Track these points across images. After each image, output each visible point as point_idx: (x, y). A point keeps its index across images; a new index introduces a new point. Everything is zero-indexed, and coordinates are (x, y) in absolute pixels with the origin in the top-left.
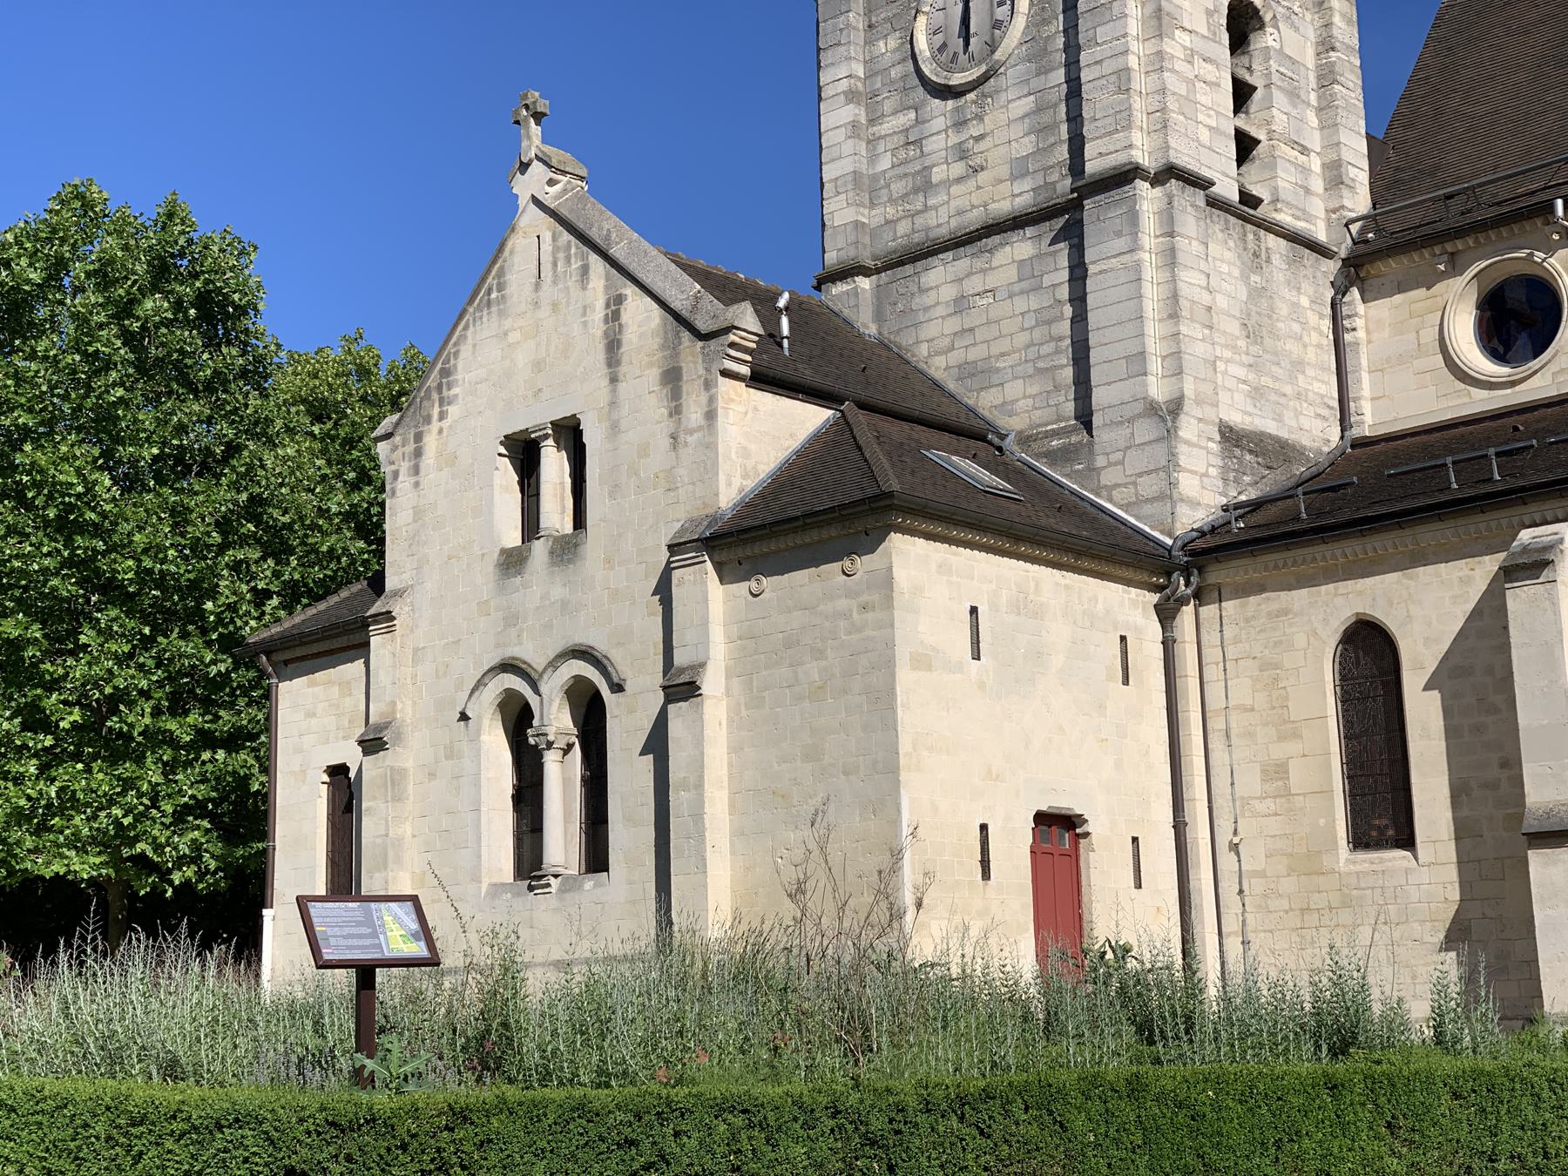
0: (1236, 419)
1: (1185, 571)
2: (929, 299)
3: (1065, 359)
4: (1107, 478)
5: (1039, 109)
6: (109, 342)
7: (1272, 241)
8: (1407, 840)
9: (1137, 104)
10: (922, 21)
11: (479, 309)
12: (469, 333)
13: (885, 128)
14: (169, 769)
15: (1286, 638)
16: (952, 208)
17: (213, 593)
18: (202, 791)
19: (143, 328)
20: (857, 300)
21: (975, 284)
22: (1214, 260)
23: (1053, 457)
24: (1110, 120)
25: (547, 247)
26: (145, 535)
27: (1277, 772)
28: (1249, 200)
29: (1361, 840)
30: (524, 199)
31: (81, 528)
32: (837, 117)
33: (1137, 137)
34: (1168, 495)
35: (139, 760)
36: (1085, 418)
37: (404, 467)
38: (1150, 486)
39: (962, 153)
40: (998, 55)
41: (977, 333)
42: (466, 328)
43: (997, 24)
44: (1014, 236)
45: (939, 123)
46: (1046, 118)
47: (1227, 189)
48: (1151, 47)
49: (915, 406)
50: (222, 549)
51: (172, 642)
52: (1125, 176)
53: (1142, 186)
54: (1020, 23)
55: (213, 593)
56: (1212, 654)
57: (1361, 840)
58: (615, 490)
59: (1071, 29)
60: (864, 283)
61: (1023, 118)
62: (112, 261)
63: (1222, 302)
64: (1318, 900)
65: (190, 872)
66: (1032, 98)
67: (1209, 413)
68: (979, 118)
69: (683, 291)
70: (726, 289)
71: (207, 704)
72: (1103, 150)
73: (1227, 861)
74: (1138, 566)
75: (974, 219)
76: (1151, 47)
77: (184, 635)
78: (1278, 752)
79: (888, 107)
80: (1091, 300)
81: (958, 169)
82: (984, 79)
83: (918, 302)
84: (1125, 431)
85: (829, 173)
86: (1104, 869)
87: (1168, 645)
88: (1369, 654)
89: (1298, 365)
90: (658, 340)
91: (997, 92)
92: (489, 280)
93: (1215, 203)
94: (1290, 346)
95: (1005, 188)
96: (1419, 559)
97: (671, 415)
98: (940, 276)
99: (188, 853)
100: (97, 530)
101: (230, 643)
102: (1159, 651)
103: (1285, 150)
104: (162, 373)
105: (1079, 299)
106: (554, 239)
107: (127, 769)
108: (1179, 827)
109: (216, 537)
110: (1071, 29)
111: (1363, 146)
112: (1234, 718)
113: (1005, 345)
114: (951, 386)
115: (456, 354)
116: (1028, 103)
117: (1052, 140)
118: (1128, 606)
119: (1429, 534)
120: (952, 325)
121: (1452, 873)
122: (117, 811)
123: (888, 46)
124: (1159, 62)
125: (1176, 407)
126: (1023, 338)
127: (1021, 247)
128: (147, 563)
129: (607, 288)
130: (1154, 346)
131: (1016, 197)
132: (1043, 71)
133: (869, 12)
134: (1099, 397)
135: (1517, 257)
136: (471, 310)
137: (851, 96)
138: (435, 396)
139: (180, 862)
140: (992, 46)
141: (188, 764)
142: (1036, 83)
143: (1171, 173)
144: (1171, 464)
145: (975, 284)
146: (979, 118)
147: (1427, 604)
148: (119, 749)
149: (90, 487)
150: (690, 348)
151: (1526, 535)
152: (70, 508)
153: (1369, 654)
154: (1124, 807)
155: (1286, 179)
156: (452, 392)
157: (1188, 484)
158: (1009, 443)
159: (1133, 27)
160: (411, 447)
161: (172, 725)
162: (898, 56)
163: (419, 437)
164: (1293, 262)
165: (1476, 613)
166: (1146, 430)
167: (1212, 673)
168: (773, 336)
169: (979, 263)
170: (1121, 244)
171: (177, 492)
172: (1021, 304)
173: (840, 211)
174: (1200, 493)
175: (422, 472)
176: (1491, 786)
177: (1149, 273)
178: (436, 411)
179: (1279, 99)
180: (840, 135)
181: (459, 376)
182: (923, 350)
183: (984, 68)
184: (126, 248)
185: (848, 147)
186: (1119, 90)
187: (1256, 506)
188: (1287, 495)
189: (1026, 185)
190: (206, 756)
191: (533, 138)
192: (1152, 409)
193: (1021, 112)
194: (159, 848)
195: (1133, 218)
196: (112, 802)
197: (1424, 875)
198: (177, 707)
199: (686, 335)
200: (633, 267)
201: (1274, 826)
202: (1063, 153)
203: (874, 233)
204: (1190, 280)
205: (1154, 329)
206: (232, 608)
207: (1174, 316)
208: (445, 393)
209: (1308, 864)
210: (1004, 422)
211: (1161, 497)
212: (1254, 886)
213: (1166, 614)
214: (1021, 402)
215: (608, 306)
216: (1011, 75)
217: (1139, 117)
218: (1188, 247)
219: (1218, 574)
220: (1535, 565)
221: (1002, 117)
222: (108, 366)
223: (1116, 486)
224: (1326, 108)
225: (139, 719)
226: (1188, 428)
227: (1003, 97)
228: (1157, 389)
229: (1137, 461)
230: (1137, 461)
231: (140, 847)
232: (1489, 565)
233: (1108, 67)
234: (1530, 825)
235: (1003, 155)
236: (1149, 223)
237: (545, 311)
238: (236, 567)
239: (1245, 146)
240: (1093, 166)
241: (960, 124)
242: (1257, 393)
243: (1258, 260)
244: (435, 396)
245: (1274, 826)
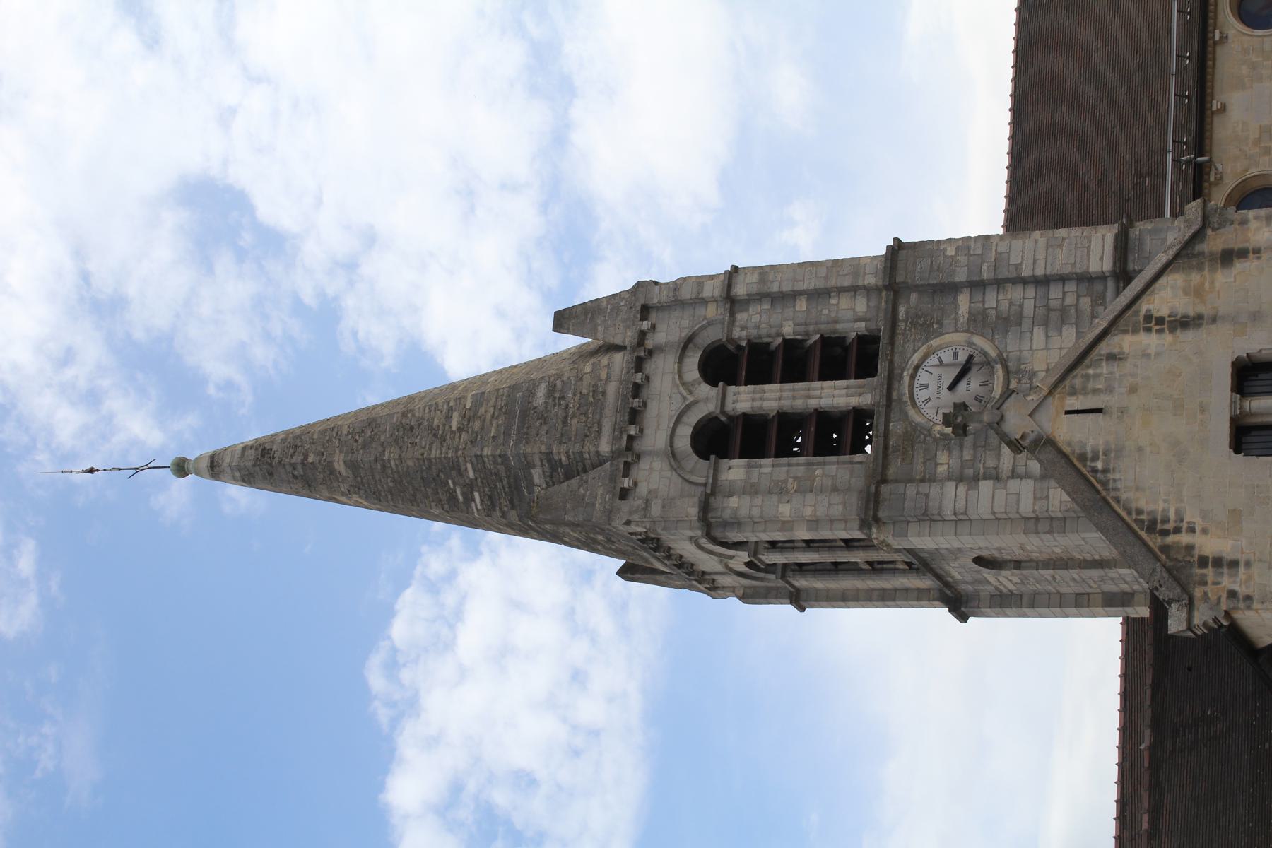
5: (1046, 323)
11: (1104, 484)
12: (1124, 496)
24: (1079, 253)
37: (1227, 582)
40: (993, 353)
42: (1118, 500)
61: (1047, 337)
66: (1036, 329)
68: (1034, 374)
72: (1098, 256)
91: (1019, 359)
92: (1084, 470)
97: (1259, 258)
106: (1073, 393)
115: (1139, 512)
116: (1039, 333)
117: (1073, 311)
129: (1135, 331)
136: (1104, 493)
138: (1171, 539)
146: (1034, 374)
156: (1172, 516)
160: (1209, 572)
162: (956, 453)
163: (1203, 562)
175: (1238, 556)
178: (1184, 538)
180: (1000, 494)
181: (1160, 506)
183: (999, 367)
186: (1060, 246)
193: (1043, 339)
199: (1199, 247)
208: (1170, 526)
215: (1148, 330)
216: (1012, 345)
227: (1026, 354)
244: (1171, 539)
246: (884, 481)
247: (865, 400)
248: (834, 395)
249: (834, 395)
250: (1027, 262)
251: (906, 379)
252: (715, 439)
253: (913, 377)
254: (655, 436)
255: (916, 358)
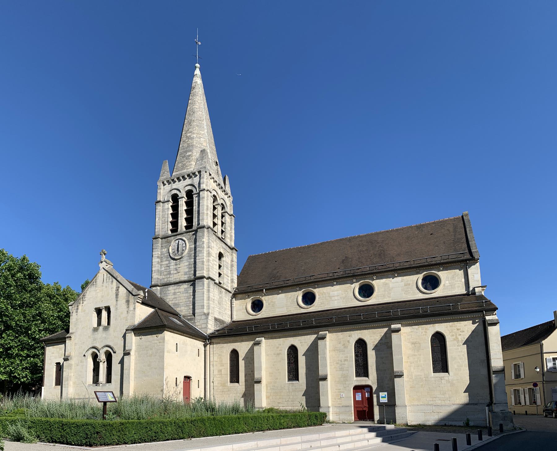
0: (216, 317)
1: (209, 340)
2: (169, 292)
3: (191, 304)
4: (197, 324)
5: (189, 265)
6: (11, 281)
7: (223, 290)
8: (238, 382)
9: (205, 267)
10: (171, 247)
13: (164, 263)
14: (21, 361)
15: (222, 352)
16: (174, 278)
17: (30, 330)
18: (28, 365)
19: (17, 279)
20: (157, 291)
21: (177, 291)
22: (215, 291)
23: (189, 320)
25: (105, 276)
26: (17, 317)
27: (220, 371)
28: (220, 283)
29: (231, 382)
30: (101, 268)
31: (5, 315)
32: (155, 260)
33: (205, 272)
34: (206, 328)
35: (14, 358)
36: (194, 314)
38: (204, 326)
39: (176, 270)
41: (177, 298)
43: (183, 250)
44: (184, 284)
45: (173, 264)
46: (190, 266)
47: (217, 281)
48: (207, 258)
49: (167, 309)
50: (33, 321)
51: (22, 337)
52: (202, 277)
53: (205, 279)
54: (187, 251)
55: (30, 330)
56: (211, 352)
57: (231, 382)
58: (116, 319)
59: (195, 253)
60: (158, 288)
62: (11, 266)
63: (215, 298)
64: (225, 390)
65: (25, 379)
67: (213, 315)
69: (131, 287)
70: (139, 288)
71: (28, 350)
73: (212, 384)
74: (201, 338)
75: (178, 280)
76: (207, 258)
77: (24, 337)
78: (221, 368)
79: (164, 260)
80: (196, 296)
81: (175, 272)
82: (181, 258)
83: (167, 292)
84: (200, 317)
85: (153, 269)
86: (194, 384)
87: (205, 351)
88: (234, 354)
89: (226, 309)
90: (125, 295)
93: (215, 283)
94: (225, 306)
95: (183, 276)
96: (242, 341)
98: (171, 288)
99: (24, 376)
100: (7, 316)
101: (34, 339)
102: (203, 352)
103: (225, 276)
104: (22, 288)
105: (194, 295)
107: (12, 360)
108: (205, 379)
109: (32, 319)
110: (195, 253)
111: (236, 277)
112: (214, 363)
113: (181, 301)
114: (172, 306)
116: (187, 263)
118: (199, 344)
119: (244, 337)
120: (173, 297)
121: (244, 387)
122: (11, 368)
123: (165, 250)
124: (208, 261)
125: (208, 314)
126: (184, 300)
127: (185, 286)
128: (18, 323)
130: (205, 304)
131: (185, 278)
132: (190, 259)
133: (162, 244)
134: (196, 311)
135: (258, 297)
137: (158, 257)
139: (23, 378)
140: (182, 253)
141: (24, 360)
142: (189, 260)
143: (209, 278)
144: (207, 323)
145: (177, 291)
147: (243, 347)
148: (10, 356)
149: (7, 308)
150: (131, 298)
151: (257, 339)
152: (3, 311)
153: (234, 354)
154: (197, 376)
155: (225, 281)
157: (209, 326)
158: (181, 317)
159: (205, 255)
161: (22, 353)
164: (226, 293)
165: (250, 349)
166: (203, 317)
167: (211, 355)
168: (145, 297)
169: (178, 287)
170: (201, 288)
171: (24, 310)
172: (184, 295)
173: (155, 276)
174: (211, 328)
176: (250, 374)
177: (205, 293)
179: (225, 268)
182: (168, 300)
184: (14, 264)
185: (157, 265)
187: (218, 331)
188: (223, 329)
189: (187, 276)
190: (29, 359)
191: (104, 258)
192: (205, 314)
194: (19, 375)
195: (203, 284)
196: (8, 366)
197: (240, 387)
198: (22, 350)
200: (121, 282)
201: (219, 379)
202: (193, 272)
203: (160, 280)
204: (211, 295)
205: (205, 301)
206: (34, 332)
207: (209, 300)
209: (224, 385)
210: (180, 313)
211: (205, 328)
212: (215, 388)
213: (205, 346)
214: (184, 310)
216: (185, 259)
217: (205, 269)
218: (211, 290)
219: (213, 341)
220: (258, 343)
221: (183, 265)
222: (11, 286)
223: (198, 325)
224: (231, 270)
225: (15, 351)
226: (210, 317)
228: (206, 311)
229: (202, 322)
230: (202, 322)
231: (15, 374)
232: (252, 343)
233: (201, 260)
234: (255, 380)
235: (183, 271)
236: (206, 285)
237: (104, 287)
238: (36, 325)
239: (220, 275)
240: (197, 275)
241: (176, 265)
242: (220, 313)
243: (221, 292)
245: (219, 379)
246: (162, 239)
247: (179, 230)
248: (182, 223)
249: (182, 223)
250: (199, 258)
251: (180, 237)
252: (175, 198)
253: (180, 239)
254: (175, 186)
255: (184, 238)
